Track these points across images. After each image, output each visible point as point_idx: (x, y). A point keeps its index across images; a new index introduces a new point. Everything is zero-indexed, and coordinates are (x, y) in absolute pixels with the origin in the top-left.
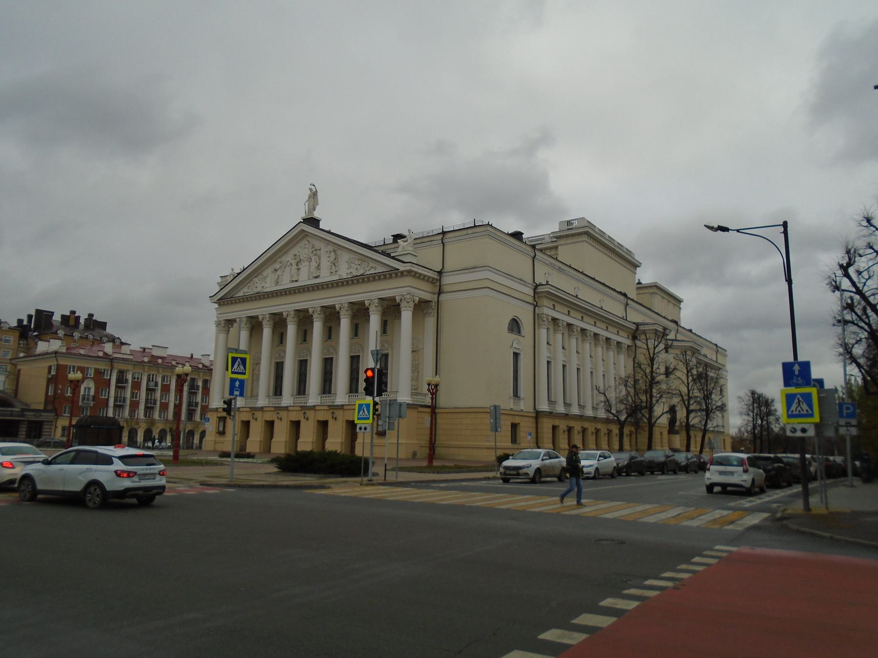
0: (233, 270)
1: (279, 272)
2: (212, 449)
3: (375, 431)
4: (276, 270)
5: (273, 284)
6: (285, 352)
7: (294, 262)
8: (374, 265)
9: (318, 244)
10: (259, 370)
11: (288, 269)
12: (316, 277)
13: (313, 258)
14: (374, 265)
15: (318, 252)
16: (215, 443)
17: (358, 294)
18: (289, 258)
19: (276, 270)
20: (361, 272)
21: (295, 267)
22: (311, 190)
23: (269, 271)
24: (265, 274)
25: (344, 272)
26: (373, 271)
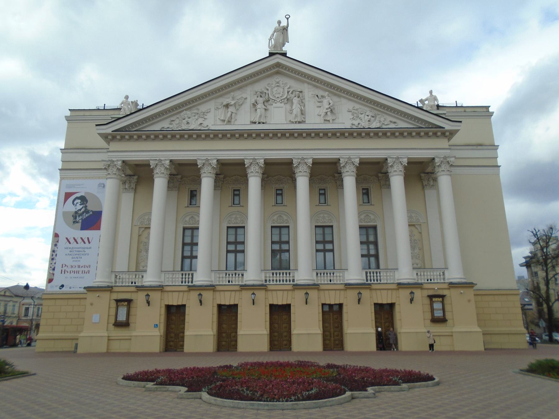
0: (127, 97)
1: (231, 109)
2: (104, 350)
3: (429, 316)
4: (227, 106)
5: (219, 122)
6: (198, 214)
7: (260, 100)
8: (394, 120)
9: (296, 86)
10: (148, 238)
11: (247, 106)
12: (299, 122)
13: (296, 100)
14: (394, 120)
15: (301, 95)
16: (109, 340)
17: (373, 150)
18: (249, 94)
19: (227, 106)
20: (375, 125)
21: (260, 106)
22: (279, 22)
23: (211, 105)
24: (203, 108)
25: (345, 121)
26: (392, 126)
